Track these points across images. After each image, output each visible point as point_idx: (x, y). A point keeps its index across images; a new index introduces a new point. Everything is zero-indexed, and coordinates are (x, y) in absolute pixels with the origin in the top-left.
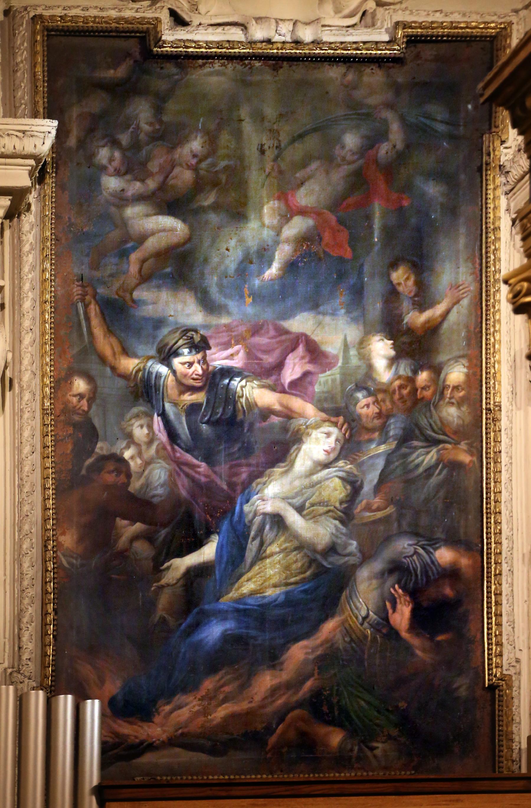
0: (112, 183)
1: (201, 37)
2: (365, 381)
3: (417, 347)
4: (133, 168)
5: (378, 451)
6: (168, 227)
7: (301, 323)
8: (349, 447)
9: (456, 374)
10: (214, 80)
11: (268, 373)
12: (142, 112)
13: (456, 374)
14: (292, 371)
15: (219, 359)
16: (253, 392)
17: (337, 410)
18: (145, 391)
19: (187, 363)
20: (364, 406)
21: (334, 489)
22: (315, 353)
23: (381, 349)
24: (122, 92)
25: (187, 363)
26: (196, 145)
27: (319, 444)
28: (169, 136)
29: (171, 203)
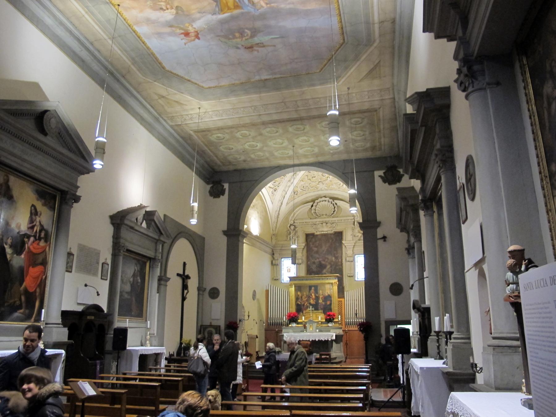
0: (311, 246)
1: (318, 233)
2: (332, 261)
3: (336, 258)
4: (313, 244)
5: (333, 267)
6: (315, 249)
7: (327, 256)
8: (331, 267)
9: (340, 260)
10: (319, 237)
11: (324, 261)
12: (313, 240)
13: (340, 260)
14: (326, 260)
15: (320, 260)
16: (323, 263)
17: (330, 263)
18: (314, 263)
19: (317, 260)
20: (332, 263)
21: (330, 270)
22: (328, 259)
23: (333, 258)
24: (312, 238)
25: (317, 260)
26: (318, 242)
27: (328, 267)
28: (316, 241)
29: (316, 247)
